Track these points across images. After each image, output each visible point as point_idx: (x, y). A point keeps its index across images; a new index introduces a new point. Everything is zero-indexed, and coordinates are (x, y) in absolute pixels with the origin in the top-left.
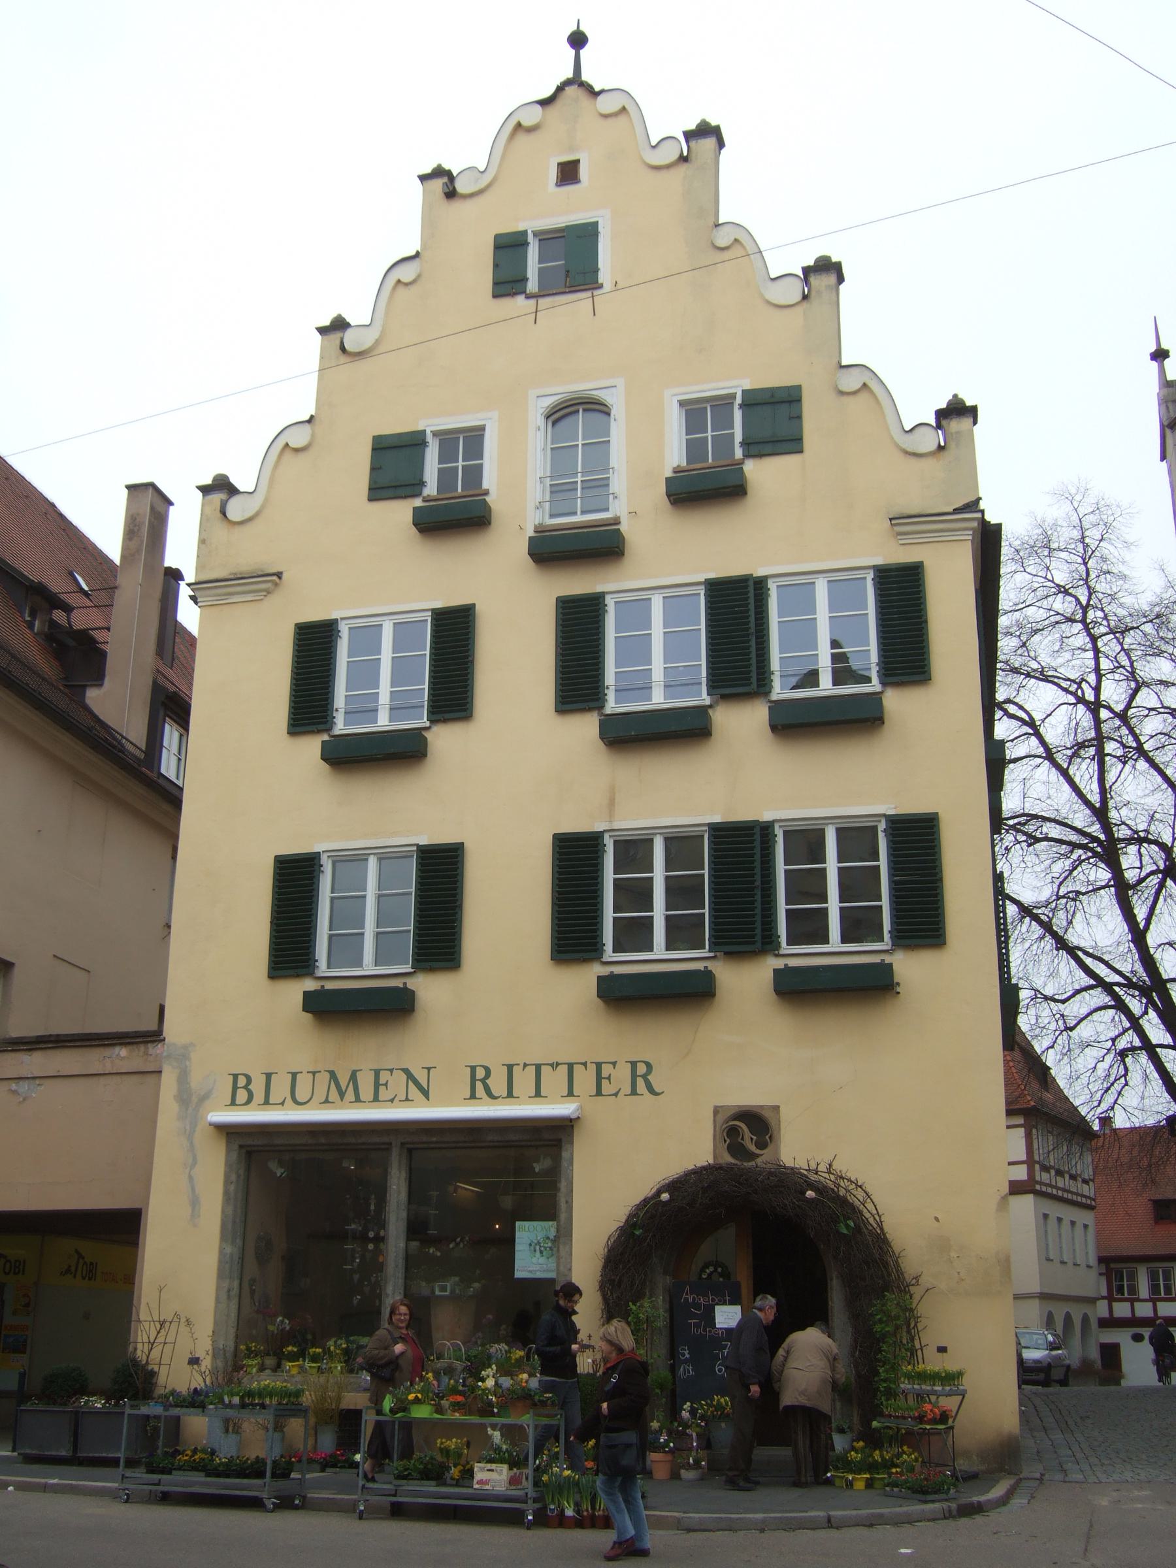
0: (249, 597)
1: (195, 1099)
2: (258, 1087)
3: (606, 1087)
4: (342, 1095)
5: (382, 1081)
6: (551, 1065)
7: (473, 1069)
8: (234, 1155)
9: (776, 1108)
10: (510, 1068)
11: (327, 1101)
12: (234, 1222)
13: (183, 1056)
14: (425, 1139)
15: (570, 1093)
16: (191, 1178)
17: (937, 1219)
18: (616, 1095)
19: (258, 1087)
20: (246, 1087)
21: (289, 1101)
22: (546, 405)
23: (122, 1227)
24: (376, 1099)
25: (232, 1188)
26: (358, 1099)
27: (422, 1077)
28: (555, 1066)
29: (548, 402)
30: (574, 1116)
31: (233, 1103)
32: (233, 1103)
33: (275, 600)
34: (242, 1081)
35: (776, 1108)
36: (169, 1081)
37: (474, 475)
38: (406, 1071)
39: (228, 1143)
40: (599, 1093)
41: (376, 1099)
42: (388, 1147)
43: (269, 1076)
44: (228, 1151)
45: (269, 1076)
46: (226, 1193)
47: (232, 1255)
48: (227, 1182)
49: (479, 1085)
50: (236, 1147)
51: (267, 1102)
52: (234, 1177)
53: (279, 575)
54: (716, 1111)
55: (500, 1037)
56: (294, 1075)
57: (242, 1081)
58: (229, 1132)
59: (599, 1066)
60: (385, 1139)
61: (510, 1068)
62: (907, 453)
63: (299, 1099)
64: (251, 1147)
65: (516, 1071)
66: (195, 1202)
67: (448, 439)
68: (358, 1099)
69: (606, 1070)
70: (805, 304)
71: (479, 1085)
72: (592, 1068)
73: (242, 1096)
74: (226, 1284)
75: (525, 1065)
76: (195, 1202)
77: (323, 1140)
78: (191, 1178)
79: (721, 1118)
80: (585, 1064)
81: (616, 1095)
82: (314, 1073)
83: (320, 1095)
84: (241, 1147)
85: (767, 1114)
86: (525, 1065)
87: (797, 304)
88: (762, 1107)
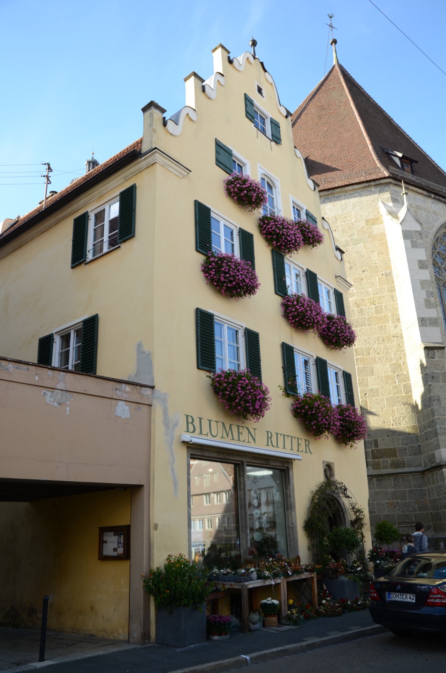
1: (171, 425)
4: (228, 435)
9: (333, 463)
11: (222, 437)
13: (164, 400)
16: (172, 470)
20: (192, 423)
21: (209, 434)
27: (252, 431)
28: (288, 436)
38: (247, 428)
45: (200, 419)
49: (269, 439)
51: (201, 433)
56: (210, 421)
61: (277, 434)
62: (336, 257)
63: (214, 433)
65: (279, 435)
66: (175, 484)
68: (233, 439)
75: (281, 434)
76: (175, 484)
78: (172, 470)
80: (295, 437)
82: (217, 422)
83: (220, 435)
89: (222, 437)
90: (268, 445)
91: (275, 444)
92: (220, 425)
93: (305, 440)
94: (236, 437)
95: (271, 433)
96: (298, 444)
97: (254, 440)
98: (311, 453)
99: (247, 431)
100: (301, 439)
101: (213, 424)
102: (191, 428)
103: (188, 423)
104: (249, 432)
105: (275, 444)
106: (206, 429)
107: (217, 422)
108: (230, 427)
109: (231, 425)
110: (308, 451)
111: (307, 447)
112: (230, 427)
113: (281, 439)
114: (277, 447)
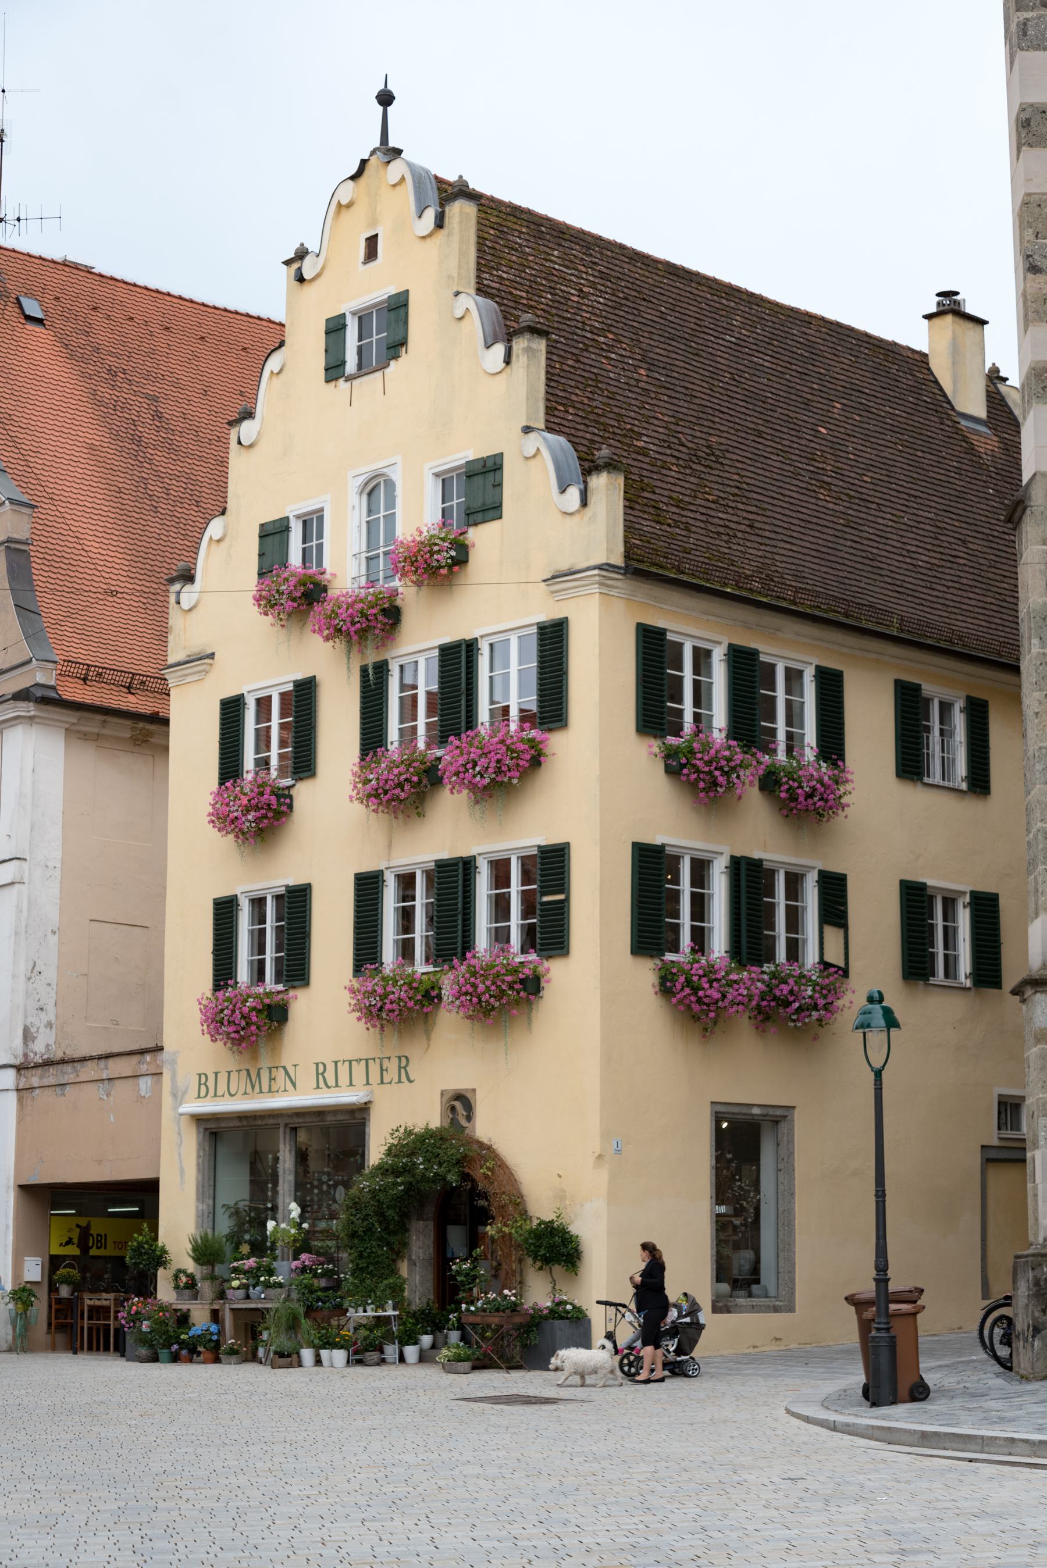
0: (196, 677)
1: (180, 1094)
2: (211, 1084)
4: (253, 1087)
9: (474, 1090)
10: (336, 1063)
11: (245, 1093)
12: (203, 1186)
14: (296, 1120)
15: (368, 1083)
16: (180, 1154)
17: (560, 1176)
19: (211, 1084)
20: (205, 1084)
21: (227, 1094)
22: (358, 484)
25: (201, 1160)
26: (261, 1092)
28: (359, 1061)
31: (199, 1097)
32: (199, 1097)
33: (211, 678)
34: (203, 1077)
35: (474, 1090)
36: (166, 1077)
38: (284, 1068)
39: (198, 1126)
40: (382, 1082)
41: (270, 1091)
42: (276, 1127)
43: (216, 1074)
44: (198, 1132)
45: (216, 1074)
46: (198, 1165)
48: (199, 1157)
50: (202, 1130)
51: (215, 1095)
52: (202, 1154)
53: (212, 656)
54: (442, 1094)
56: (229, 1073)
58: (199, 1119)
59: (381, 1059)
61: (336, 1063)
63: (233, 1092)
65: (339, 1064)
66: (182, 1172)
68: (261, 1092)
69: (386, 1063)
70: (508, 369)
73: (203, 1087)
76: (182, 1172)
77: (245, 1123)
78: (180, 1154)
79: (446, 1097)
80: (374, 1059)
84: (206, 1129)
85: (469, 1096)
89: (245, 1093)
90: (318, 1087)
91: (331, 1082)
93: (399, 1058)
94: (265, 1088)
96: (382, 1070)
97: (294, 1085)
98: (411, 1081)
100: (389, 1058)
101: (234, 1076)
102: (203, 1094)
103: (200, 1084)
104: (287, 1073)
105: (331, 1082)
106: (222, 1088)
107: (239, 1071)
110: (404, 1078)
112: (259, 1075)
113: (343, 1070)
114: (337, 1085)
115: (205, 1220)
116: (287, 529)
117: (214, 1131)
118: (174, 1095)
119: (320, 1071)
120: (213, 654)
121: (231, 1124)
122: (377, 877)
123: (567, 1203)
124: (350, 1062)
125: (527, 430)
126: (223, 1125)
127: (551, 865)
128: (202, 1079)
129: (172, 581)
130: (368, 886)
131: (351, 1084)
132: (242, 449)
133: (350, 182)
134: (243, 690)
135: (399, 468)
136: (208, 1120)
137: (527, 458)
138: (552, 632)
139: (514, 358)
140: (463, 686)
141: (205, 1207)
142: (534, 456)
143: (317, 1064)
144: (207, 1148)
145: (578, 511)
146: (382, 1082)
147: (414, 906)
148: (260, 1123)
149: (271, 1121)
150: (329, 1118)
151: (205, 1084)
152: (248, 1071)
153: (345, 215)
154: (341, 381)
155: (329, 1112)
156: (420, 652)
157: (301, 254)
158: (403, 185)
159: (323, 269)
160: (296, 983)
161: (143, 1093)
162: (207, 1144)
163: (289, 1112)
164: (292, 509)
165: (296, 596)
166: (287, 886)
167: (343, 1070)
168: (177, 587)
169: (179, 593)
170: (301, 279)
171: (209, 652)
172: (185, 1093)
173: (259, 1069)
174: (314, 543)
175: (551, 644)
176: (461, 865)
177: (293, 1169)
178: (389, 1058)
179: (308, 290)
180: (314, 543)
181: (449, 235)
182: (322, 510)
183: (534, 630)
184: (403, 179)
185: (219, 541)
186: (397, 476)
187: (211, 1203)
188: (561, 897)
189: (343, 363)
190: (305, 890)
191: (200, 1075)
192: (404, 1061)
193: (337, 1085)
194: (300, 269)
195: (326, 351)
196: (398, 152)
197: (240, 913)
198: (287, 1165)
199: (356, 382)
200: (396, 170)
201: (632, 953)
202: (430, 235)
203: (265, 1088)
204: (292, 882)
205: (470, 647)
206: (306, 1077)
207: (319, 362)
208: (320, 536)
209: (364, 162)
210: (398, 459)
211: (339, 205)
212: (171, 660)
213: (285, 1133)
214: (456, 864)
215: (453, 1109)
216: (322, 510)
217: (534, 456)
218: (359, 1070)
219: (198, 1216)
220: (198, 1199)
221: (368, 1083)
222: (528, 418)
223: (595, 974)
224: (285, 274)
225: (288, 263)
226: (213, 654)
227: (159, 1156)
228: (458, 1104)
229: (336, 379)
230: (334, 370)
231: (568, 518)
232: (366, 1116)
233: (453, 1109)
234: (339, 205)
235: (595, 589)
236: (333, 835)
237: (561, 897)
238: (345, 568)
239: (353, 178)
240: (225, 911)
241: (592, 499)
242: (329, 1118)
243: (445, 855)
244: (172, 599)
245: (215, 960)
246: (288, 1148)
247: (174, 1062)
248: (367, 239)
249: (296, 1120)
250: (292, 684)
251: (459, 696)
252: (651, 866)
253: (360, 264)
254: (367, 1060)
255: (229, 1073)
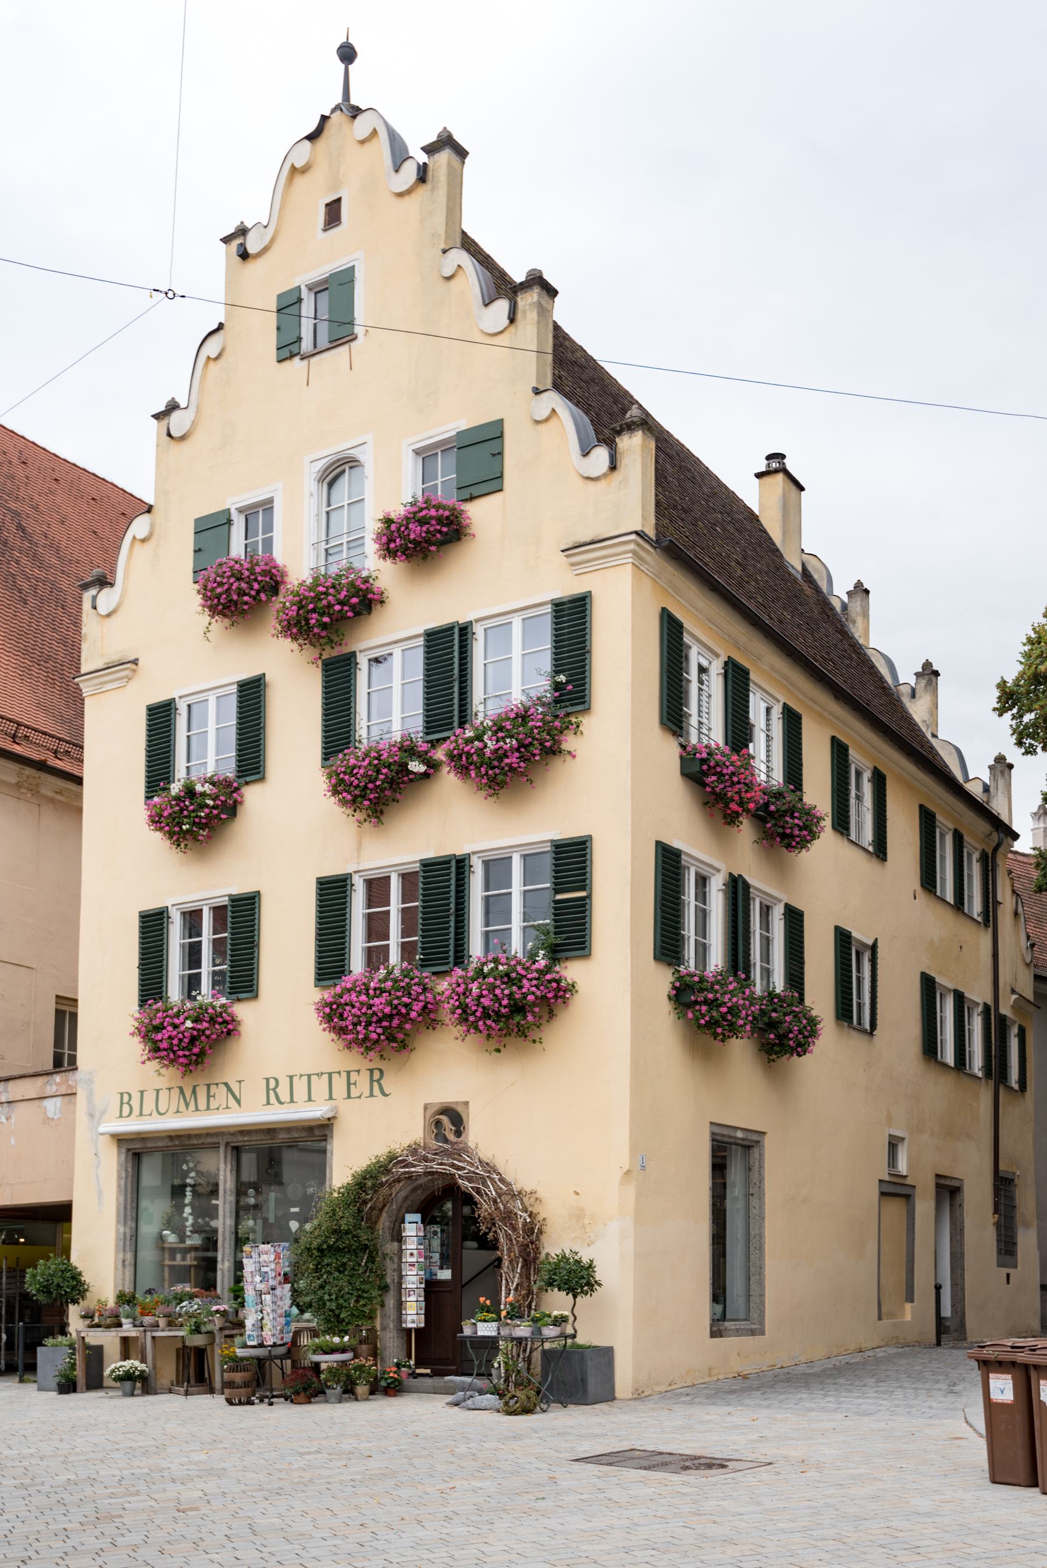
1: (97, 1114)
2: (135, 1102)
3: (354, 1092)
4: (187, 1105)
5: (212, 1094)
6: (317, 1074)
7: (268, 1080)
8: (123, 1156)
9: (467, 1103)
10: (291, 1078)
11: (178, 1112)
12: (125, 1208)
15: (331, 1098)
16: (97, 1176)
18: (360, 1097)
19: (135, 1102)
20: (128, 1103)
21: (155, 1112)
22: (317, 469)
23: (60, 1214)
24: (208, 1109)
25: (123, 1182)
26: (197, 1109)
28: (320, 1075)
29: (320, 465)
30: (329, 1115)
31: (121, 1116)
32: (121, 1116)
34: (126, 1098)
35: (467, 1103)
37: (268, 543)
38: (226, 1084)
39: (119, 1146)
40: (349, 1097)
41: (208, 1109)
43: (142, 1092)
44: (119, 1152)
45: (142, 1092)
46: (119, 1186)
47: (125, 1234)
48: (119, 1178)
49: (271, 1092)
50: (124, 1150)
51: (141, 1114)
52: (123, 1174)
54: (426, 1108)
55: (284, 1053)
56: (158, 1091)
57: (126, 1098)
58: (121, 1140)
59: (348, 1073)
60: (215, 1140)
61: (291, 1078)
63: (162, 1111)
64: (136, 1150)
66: (100, 1194)
67: (250, 512)
68: (197, 1109)
69: (354, 1077)
70: (512, 329)
71: (271, 1092)
72: (344, 1075)
74: (121, 1256)
75: (301, 1076)
77: (177, 1143)
79: (430, 1112)
80: (339, 1073)
81: (360, 1097)
82: (169, 1089)
84: (129, 1150)
85: (460, 1109)
86: (301, 1076)
87: (506, 329)
88: (457, 1103)
89: (178, 1112)
90: (268, 1103)
91: (284, 1096)
92: (176, 1092)
93: (371, 1071)
94: (202, 1104)
95: (277, 1080)
96: (349, 1084)
97: (238, 1101)
98: (385, 1095)
99: (225, 1089)
100: (358, 1071)
101: (164, 1094)
103: (122, 1104)
105: (284, 1096)
106: (149, 1105)
107: (169, 1089)
108: (194, 1092)
109: (194, 1087)
111: (375, 1084)
112: (194, 1092)
113: (300, 1086)
115: (128, 1243)
116: (229, 522)
117: (136, 1150)
118: (91, 1116)
119: (271, 1087)
120: (137, 660)
121: (160, 1144)
122: (345, 880)
123: (586, 1222)
124: (309, 1076)
125: (537, 392)
126: (149, 1145)
127: (571, 860)
128: (125, 1099)
129: (86, 587)
130: (332, 893)
131: (310, 1099)
132: (172, 443)
133: (307, 142)
134: (175, 695)
135: (369, 448)
136: (132, 1140)
137: (537, 422)
138: (570, 608)
139: (519, 316)
140: (456, 671)
141: (128, 1230)
142: (547, 420)
143: (268, 1080)
144: (130, 1170)
145: (605, 475)
146: (349, 1097)
147: (388, 912)
148: (195, 1142)
149: (209, 1140)
150: (281, 1136)
151: (128, 1103)
152: (181, 1089)
153: (300, 181)
154: (297, 359)
155: (281, 1129)
156: (396, 642)
157: (242, 231)
158: (374, 141)
159: (272, 241)
160: (241, 996)
161: (50, 1115)
162: (130, 1165)
163: (232, 1130)
164: (234, 499)
165: (239, 593)
166: (230, 896)
167: (300, 1086)
168: (93, 592)
169: (94, 598)
170: (244, 255)
171: (132, 658)
172: (104, 1112)
173: (194, 1087)
174: (260, 537)
175: (569, 621)
176: (453, 863)
177: (234, 1190)
178: (358, 1071)
179: (252, 266)
180: (260, 537)
181: (433, 189)
182: (271, 501)
183: (548, 609)
184: (375, 132)
185: (143, 541)
186: (364, 456)
187: (133, 1225)
188: (583, 894)
189: (299, 339)
190: (253, 898)
191: (122, 1094)
192: (377, 1075)
193: (292, 1101)
194: (242, 245)
195: (278, 329)
196: (356, 112)
197: (171, 926)
198: (228, 1185)
199: (313, 360)
200: (362, 126)
201: (655, 958)
202: (409, 192)
203: (202, 1104)
204: (236, 890)
205: (465, 631)
206: (253, 1092)
207: (270, 341)
208: (269, 527)
209: (324, 119)
210: (369, 438)
211: (294, 169)
212: (83, 671)
213: (226, 1153)
214: (449, 862)
215: (438, 1123)
216: (271, 501)
217: (547, 420)
218: (320, 1086)
219: (117, 1239)
220: (118, 1222)
221: (331, 1098)
222: (538, 380)
223: (615, 979)
224: (221, 255)
225: (226, 240)
226: (137, 660)
227: (71, 1179)
228: (445, 1119)
229: (292, 356)
230: (288, 349)
231: (591, 485)
232: (327, 1133)
233: (438, 1123)
234: (294, 169)
235: (629, 559)
236: (294, 836)
237: (583, 894)
238: (299, 559)
239: (312, 137)
240: (153, 924)
241: (624, 462)
242: (281, 1136)
243: (430, 854)
244: (87, 605)
245: (141, 975)
246: (229, 1167)
247: (90, 1081)
248: (327, 205)
249: (240, 1138)
250: (235, 686)
251: (451, 682)
252: (669, 863)
253: (321, 232)
254: (330, 1074)
255: (158, 1091)
